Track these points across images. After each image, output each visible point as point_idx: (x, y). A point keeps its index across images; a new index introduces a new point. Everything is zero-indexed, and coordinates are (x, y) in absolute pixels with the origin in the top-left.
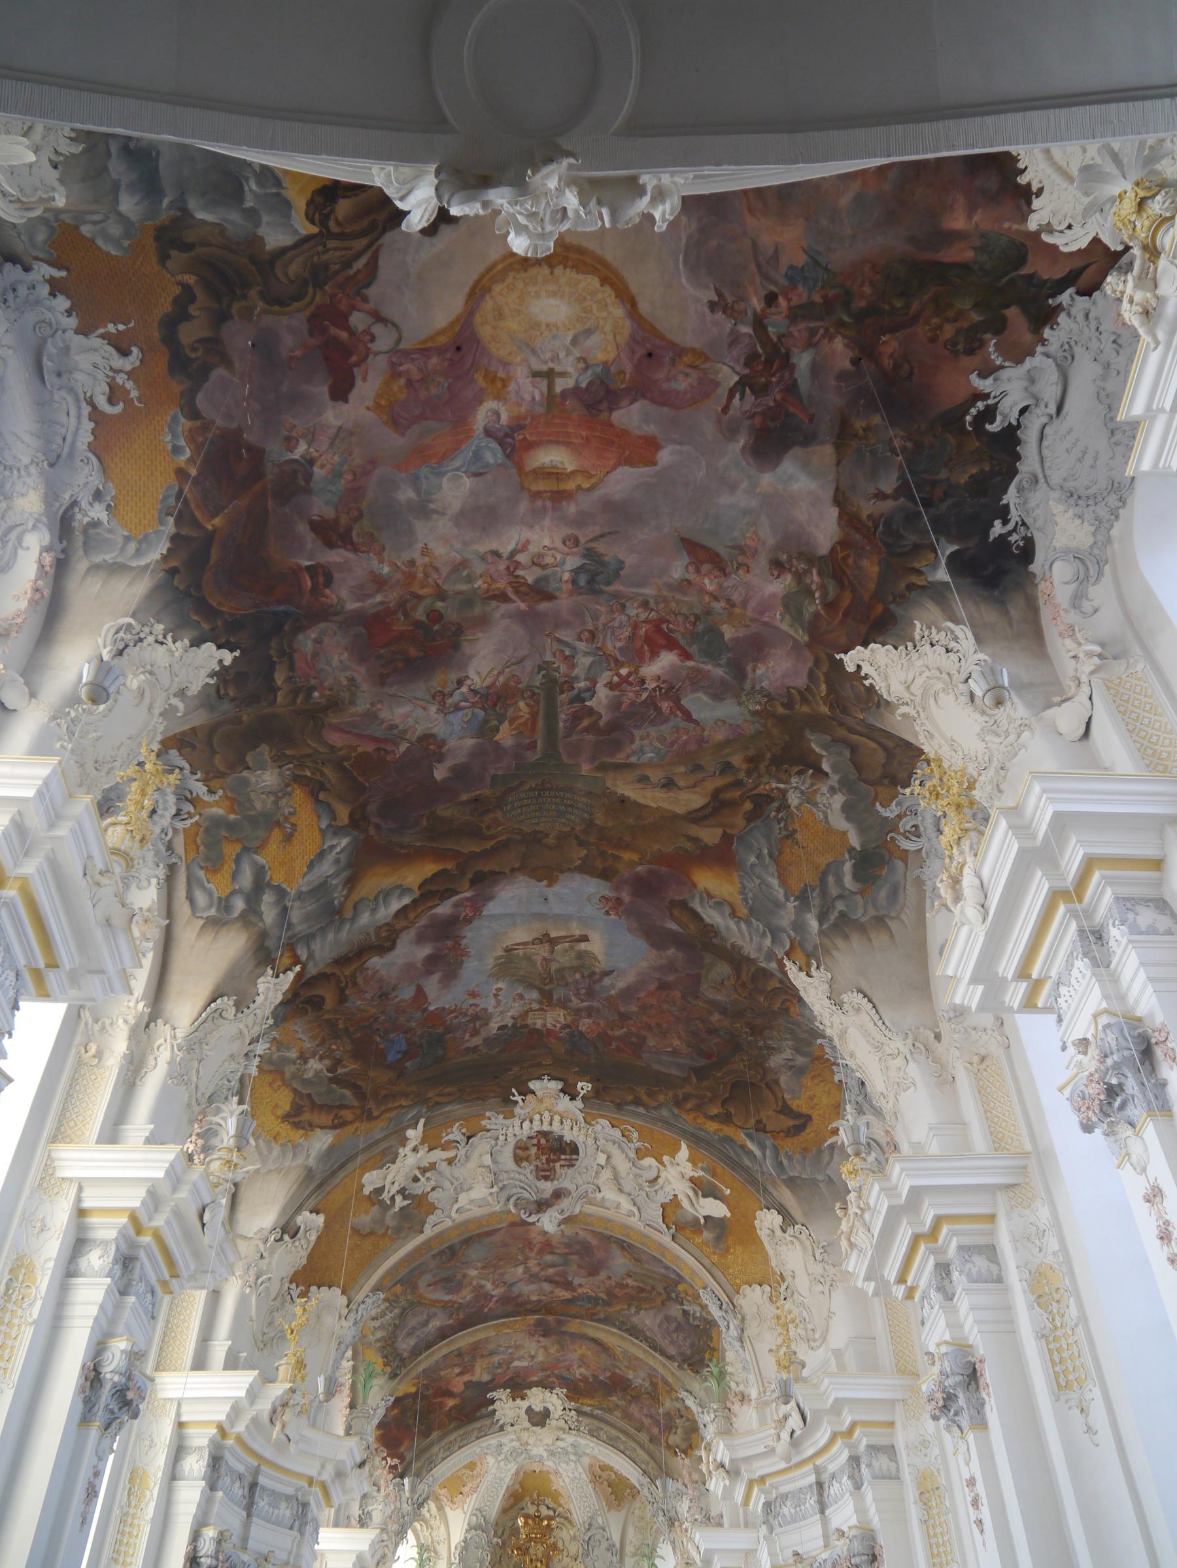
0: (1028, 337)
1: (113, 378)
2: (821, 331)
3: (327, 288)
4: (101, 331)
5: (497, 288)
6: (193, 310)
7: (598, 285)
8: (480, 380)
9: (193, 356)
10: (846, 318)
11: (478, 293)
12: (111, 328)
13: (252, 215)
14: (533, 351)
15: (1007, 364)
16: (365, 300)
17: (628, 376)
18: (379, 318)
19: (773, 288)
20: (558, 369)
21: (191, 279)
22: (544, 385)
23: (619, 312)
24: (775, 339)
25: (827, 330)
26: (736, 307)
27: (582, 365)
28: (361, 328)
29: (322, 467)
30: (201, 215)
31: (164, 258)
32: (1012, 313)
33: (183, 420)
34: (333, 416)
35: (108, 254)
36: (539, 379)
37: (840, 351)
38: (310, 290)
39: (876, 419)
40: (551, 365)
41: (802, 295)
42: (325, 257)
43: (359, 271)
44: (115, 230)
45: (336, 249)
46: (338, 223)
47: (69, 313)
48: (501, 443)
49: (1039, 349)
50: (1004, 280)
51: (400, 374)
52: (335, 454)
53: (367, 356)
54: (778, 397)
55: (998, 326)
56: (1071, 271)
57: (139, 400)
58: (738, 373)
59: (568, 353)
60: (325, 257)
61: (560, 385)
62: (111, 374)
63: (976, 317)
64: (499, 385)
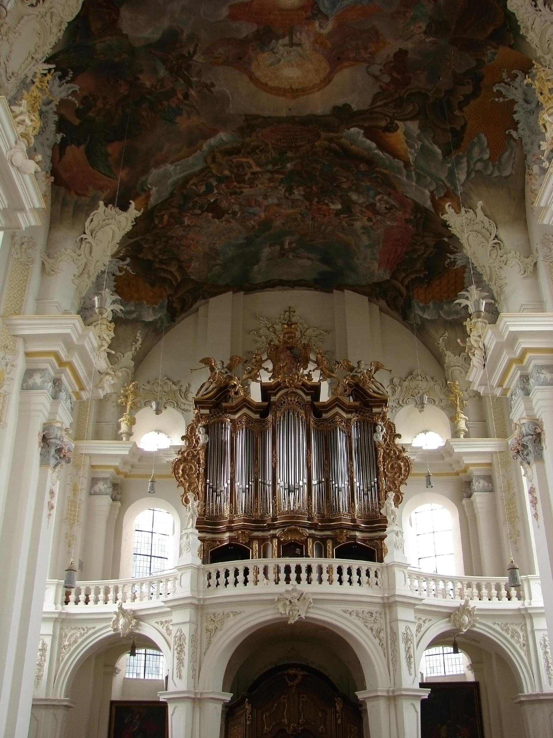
0: (63, 112)
1: (511, 81)
2: (158, 88)
3: (397, 96)
4: (506, 100)
5: (317, 82)
6: (462, 98)
7: (269, 83)
8: (329, 44)
9: (469, 80)
10: (149, 97)
11: (327, 80)
12: (501, 100)
13: (419, 138)
14: (300, 55)
15: (66, 98)
16: (381, 87)
17: (251, 48)
18: (376, 78)
19: (186, 102)
20: (288, 48)
21: (457, 113)
22: (295, 40)
23: (258, 74)
24: (180, 79)
25: (156, 89)
26: (201, 87)
27: (275, 51)
28: (386, 76)
29: (420, 27)
30: (439, 151)
31: (463, 128)
32: (77, 122)
33: (486, 61)
34: (409, 45)
35: (485, 136)
36: (298, 43)
37: (147, 82)
38: (405, 96)
39: (117, 60)
40: (291, 49)
41: (173, 103)
42: (394, 111)
43: (381, 100)
44: (476, 150)
45: (389, 112)
46: (386, 120)
47: (515, 112)
48: (319, 11)
49: (55, 110)
50: (89, 138)
51: (370, 53)
52: (412, 31)
53: (385, 64)
54: (170, 56)
55: (78, 113)
56: (65, 153)
57: (504, 72)
58: (194, 61)
59: (282, 55)
60: (394, 111)
61: (286, 40)
62: (511, 83)
63: (90, 114)
64: (319, 41)
